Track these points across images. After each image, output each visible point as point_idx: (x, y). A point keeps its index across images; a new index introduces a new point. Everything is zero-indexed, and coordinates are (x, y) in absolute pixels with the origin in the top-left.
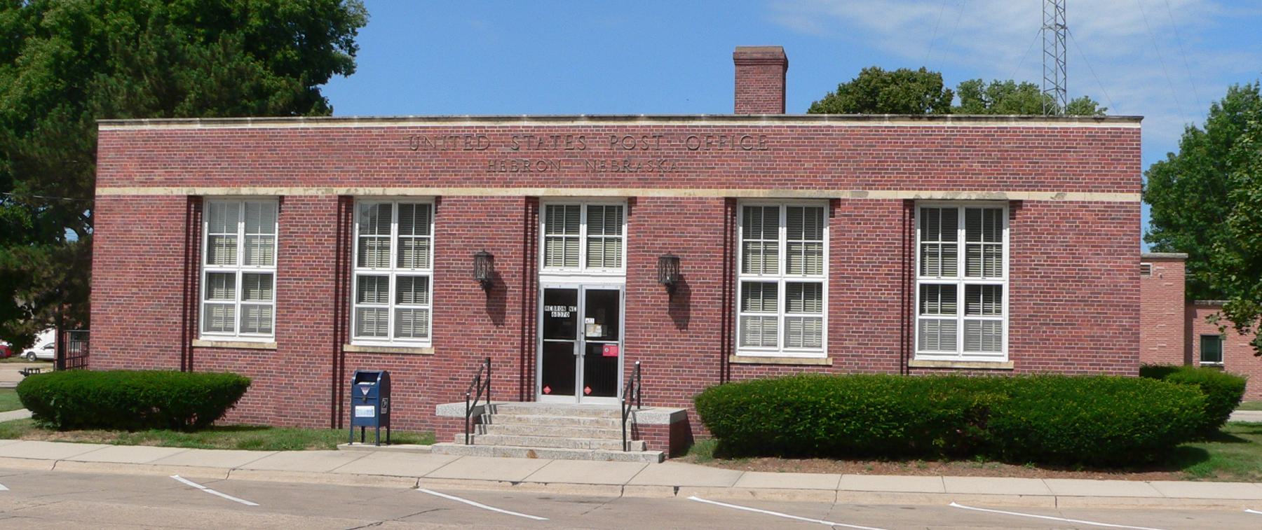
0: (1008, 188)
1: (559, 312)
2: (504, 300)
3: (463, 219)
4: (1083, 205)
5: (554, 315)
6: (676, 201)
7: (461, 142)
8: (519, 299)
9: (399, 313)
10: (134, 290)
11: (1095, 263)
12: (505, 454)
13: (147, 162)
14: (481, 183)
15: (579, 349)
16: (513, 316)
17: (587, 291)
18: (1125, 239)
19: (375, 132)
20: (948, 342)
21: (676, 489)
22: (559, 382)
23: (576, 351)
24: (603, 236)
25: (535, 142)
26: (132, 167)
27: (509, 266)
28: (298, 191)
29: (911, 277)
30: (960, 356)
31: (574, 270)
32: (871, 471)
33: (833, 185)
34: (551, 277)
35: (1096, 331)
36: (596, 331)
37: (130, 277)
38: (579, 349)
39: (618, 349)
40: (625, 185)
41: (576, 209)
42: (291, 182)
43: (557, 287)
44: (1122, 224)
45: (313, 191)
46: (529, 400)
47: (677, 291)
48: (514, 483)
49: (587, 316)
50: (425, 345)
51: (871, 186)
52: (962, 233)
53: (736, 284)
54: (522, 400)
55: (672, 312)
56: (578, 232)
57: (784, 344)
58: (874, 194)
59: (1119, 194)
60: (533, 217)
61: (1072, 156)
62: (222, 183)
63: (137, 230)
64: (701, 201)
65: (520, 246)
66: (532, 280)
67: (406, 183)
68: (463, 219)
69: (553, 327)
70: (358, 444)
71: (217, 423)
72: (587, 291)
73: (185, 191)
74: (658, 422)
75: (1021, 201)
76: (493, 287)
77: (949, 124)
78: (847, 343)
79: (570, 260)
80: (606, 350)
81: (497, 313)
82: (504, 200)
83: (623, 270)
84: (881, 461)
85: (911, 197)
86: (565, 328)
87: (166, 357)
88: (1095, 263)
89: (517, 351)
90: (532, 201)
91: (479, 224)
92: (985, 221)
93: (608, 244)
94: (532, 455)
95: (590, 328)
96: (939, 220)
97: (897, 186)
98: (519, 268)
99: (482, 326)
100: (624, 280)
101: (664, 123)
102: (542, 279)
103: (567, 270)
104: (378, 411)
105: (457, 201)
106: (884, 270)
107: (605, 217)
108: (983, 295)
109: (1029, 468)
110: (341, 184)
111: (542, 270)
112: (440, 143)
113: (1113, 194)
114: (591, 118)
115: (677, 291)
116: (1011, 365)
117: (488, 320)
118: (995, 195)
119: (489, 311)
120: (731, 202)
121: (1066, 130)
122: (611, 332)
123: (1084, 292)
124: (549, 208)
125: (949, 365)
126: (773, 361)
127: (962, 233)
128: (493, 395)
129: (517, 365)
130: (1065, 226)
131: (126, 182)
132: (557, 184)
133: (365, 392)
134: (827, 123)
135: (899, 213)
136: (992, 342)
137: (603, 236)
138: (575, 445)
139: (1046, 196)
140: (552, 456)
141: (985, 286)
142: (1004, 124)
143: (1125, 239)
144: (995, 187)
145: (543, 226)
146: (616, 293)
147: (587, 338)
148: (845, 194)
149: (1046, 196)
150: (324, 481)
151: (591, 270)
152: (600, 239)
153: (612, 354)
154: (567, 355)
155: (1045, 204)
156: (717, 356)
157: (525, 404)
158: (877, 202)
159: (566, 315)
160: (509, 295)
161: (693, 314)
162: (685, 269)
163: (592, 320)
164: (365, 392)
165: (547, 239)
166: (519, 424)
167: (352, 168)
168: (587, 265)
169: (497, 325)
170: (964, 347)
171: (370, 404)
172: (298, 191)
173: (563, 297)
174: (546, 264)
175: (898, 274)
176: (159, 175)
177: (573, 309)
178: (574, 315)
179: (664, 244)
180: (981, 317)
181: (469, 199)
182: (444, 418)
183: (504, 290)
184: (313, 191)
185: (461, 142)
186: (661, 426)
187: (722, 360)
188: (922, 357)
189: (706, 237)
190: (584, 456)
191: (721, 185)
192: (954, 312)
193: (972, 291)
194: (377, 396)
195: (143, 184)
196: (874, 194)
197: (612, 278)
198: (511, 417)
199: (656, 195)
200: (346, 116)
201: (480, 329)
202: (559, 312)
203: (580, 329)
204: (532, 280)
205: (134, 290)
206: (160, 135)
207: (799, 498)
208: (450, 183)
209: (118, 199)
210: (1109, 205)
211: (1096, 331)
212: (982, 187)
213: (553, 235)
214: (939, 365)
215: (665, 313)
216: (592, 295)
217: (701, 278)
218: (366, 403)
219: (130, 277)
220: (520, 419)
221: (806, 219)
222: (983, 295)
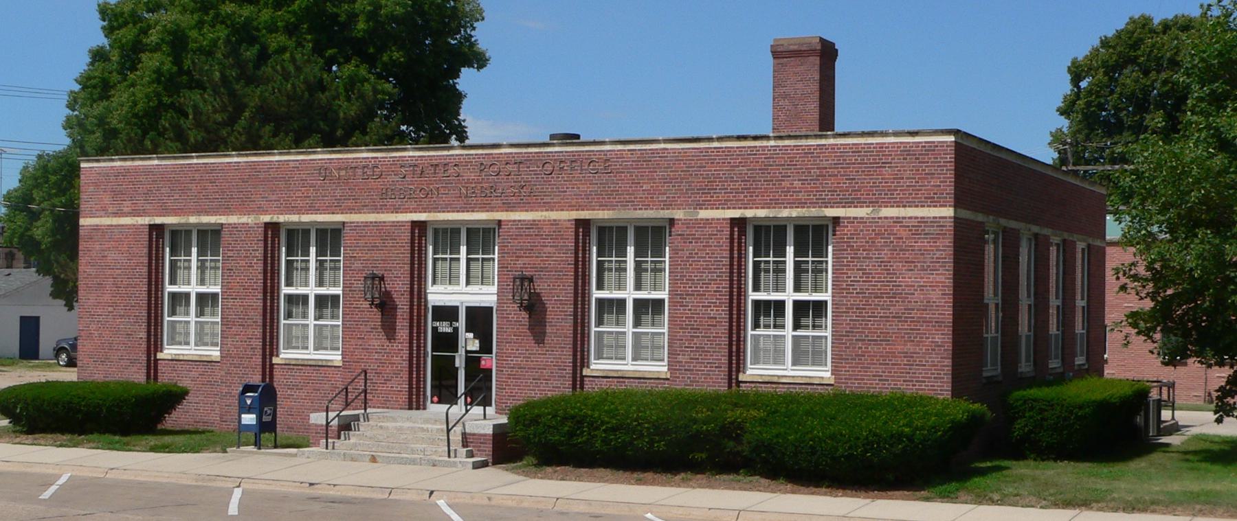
0: (826, 205)
1: (445, 328)
2: (394, 316)
3: (361, 243)
4: (898, 220)
5: (441, 330)
6: (534, 224)
7: (359, 172)
8: (406, 316)
9: (319, 329)
11: (908, 278)
12: (352, 460)
13: (117, 194)
14: (376, 209)
15: (460, 362)
16: (402, 333)
18: (938, 254)
19: (292, 164)
20: (778, 358)
21: (432, 493)
22: (445, 393)
23: (457, 365)
24: (480, 256)
25: (418, 170)
26: (107, 199)
27: (398, 286)
28: (233, 219)
29: (742, 293)
30: (788, 371)
32: (639, 482)
33: (668, 206)
34: (438, 295)
35: (910, 347)
36: (474, 345)
37: (107, 297)
38: (460, 362)
39: (490, 361)
40: (491, 209)
41: (458, 231)
42: (227, 211)
43: (441, 304)
44: (935, 240)
46: (418, 409)
47: (534, 307)
48: (311, 484)
49: (467, 331)
50: (336, 357)
51: (701, 206)
52: (790, 250)
53: (589, 301)
54: (410, 408)
55: (531, 328)
56: (459, 253)
57: (632, 359)
58: (704, 214)
59: (932, 209)
60: (420, 240)
61: (887, 171)
62: (175, 213)
63: (112, 256)
64: (555, 223)
65: (407, 267)
66: (419, 298)
67: (318, 211)
68: (361, 243)
70: (251, 448)
73: (146, 220)
74: (482, 432)
75: (838, 218)
76: (385, 305)
78: (680, 358)
79: (452, 279)
80: (483, 362)
81: (389, 330)
82: (396, 224)
84: (656, 472)
85: (737, 216)
86: (447, 342)
87: (134, 369)
88: (908, 278)
89: (406, 364)
90: (419, 226)
91: (374, 248)
92: (812, 237)
93: (486, 263)
94: (374, 459)
96: (769, 236)
97: (725, 205)
98: (407, 288)
99: (377, 341)
100: (495, 298)
101: (524, 150)
102: (430, 297)
103: (450, 288)
104: (259, 418)
105: (357, 226)
106: (713, 287)
107: (481, 238)
108: (807, 312)
109: (781, 484)
110: (266, 212)
111: (431, 289)
112: (343, 173)
113: (926, 209)
115: (534, 307)
117: (382, 336)
118: (813, 212)
119: (383, 327)
120: (583, 225)
121: (881, 145)
122: (486, 347)
123: (898, 308)
124: (436, 231)
125: (775, 380)
126: (620, 374)
127: (790, 250)
128: (370, 403)
129: (406, 376)
130: (880, 242)
131: (102, 213)
132: (436, 209)
133: (249, 402)
135: (727, 232)
136: (818, 359)
137: (480, 256)
138: (413, 451)
139: (862, 212)
140: (389, 461)
141: (814, 302)
142: (823, 142)
143: (938, 254)
145: (430, 248)
146: (491, 309)
147: (467, 352)
148: (678, 214)
149: (862, 212)
150: (173, 481)
151: (471, 289)
152: (446, 259)
153: (488, 366)
154: (444, 366)
155: (861, 220)
156: (569, 370)
157: (414, 412)
158: (707, 222)
159: (449, 330)
160: (399, 312)
161: (549, 330)
162: (541, 286)
163: (471, 335)
164: (249, 402)
165: (435, 260)
166: (381, 432)
168: (468, 283)
169: (389, 339)
170: (783, 362)
171: (266, 414)
172: (233, 219)
173: (446, 313)
174: (434, 282)
175: (726, 291)
177: (456, 324)
178: (456, 329)
179: (522, 264)
180: (810, 333)
181: (367, 224)
182: (316, 425)
183: (395, 308)
185: (359, 172)
186: (485, 435)
187: (574, 373)
188: (754, 371)
189: (560, 256)
190: (413, 462)
191: (572, 207)
192: (783, 327)
193: (800, 307)
194: (257, 405)
195: (116, 214)
196: (704, 214)
197: (486, 295)
198: (389, 424)
199: (517, 218)
201: (376, 343)
203: (461, 343)
204: (419, 298)
205: (110, 309)
206: (127, 171)
207: (525, 504)
208: (351, 210)
209: (96, 228)
210: (923, 220)
211: (910, 347)
212: (802, 204)
213: (440, 256)
214: (767, 379)
215: (525, 329)
216: (471, 311)
217: (556, 295)
218: (249, 412)
219: (107, 297)
220: (381, 427)
222: (807, 312)
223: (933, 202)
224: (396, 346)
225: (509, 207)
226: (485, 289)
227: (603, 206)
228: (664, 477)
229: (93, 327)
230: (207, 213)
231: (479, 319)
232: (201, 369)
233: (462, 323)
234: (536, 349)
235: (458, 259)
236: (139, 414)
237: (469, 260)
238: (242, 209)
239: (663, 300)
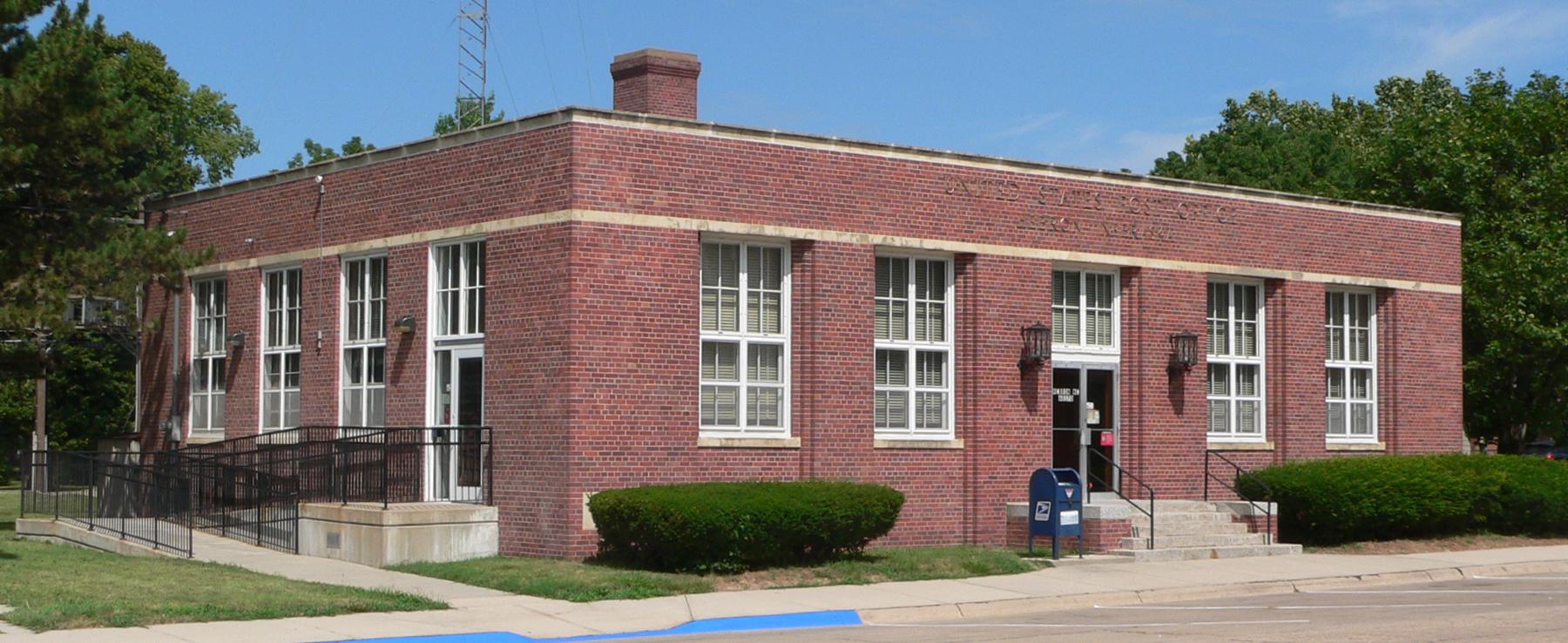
1: (1065, 396)
4: (1431, 294)
5: (1062, 399)
6: (1171, 274)
10: (631, 366)
11: (1438, 350)
12: (1194, 558)
14: (1014, 241)
17: (1089, 372)
19: (910, 167)
26: (623, 182)
28: (830, 236)
31: (1086, 347)
33: (1280, 266)
34: (1063, 354)
36: (1094, 418)
39: (1113, 437)
42: (823, 222)
45: (846, 237)
51: (1304, 268)
62: (742, 217)
63: (633, 277)
64: (1190, 274)
69: (1066, 415)
71: (875, 546)
72: (1089, 372)
73: (693, 224)
77: (1352, 210)
82: (1035, 262)
83: (1116, 348)
86: (1066, 415)
87: (676, 464)
94: (1214, 555)
95: (1090, 415)
99: (1017, 413)
100: (1117, 360)
102: (1054, 357)
103: (1073, 347)
110: (876, 230)
111: (1055, 346)
116: (1382, 446)
119: (1023, 395)
122: (1106, 421)
131: (616, 205)
134: (1275, 201)
140: (1229, 554)
144: (1380, 275)
146: (1110, 373)
148: (1288, 275)
159: (1070, 399)
163: (1091, 405)
167: (888, 210)
172: (830, 236)
173: (1066, 377)
176: (660, 197)
177: (1077, 392)
178: (1077, 398)
181: (1003, 260)
182: (1109, 521)
184: (846, 237)
195: (643, 208)
197: (1108, 355)
200: (1087, 168)
201: (1015, 416)
202: (1065, 396)
205: (631, 366)
206: (659, 140)
208: (985, 239)
209: (604, 229)
211: (1438, 414)
216: (1092, 373)
219: (624, 347)
221: (1248, 296)
223: (1451, 282)
224: (1038, 420)
225: (1149, 253)
226: (1106, 349)
227: (1231, 261)
228: (1421, 544)
229: (600, 395)
230: (792, 222)
231: (1100, 382)
232: (765, 460)
233: (1083, 391)
234: (1176, 421)
235: (1078, 312)
236: (818, 530)
237: (1089, 312)
238: (845, 224)
239: (1370, 370)
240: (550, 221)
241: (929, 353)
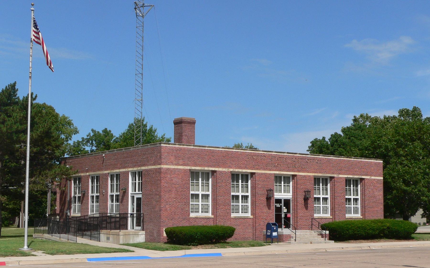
1: (278, 205)
4: (374, 179)
5: (277, 206)
6: (305, 176)
10: (174, 200)
11: (376, 193)
12: (306, 243)
13: (177, 158)
17: (284, 200)
19: (239, 153)
26: (172, 159)
28: (220, 169)
31: (283, 193)
33: (333, 173)
34: (277, 195)
37: (173, 195)
39: (290, 215)
42: (219, 166)
45: (224, 170)
51: (340, 174)
58: (341, 176)
61: (372, 168)
62: (200, 166)
63: (175, 180)
64: (309, 176)
69: (278, 210)
71: (228, 240)
72: (284, 200)
73: (188, 168)
77: (353, 159)
79: (280, 191)
82: (270, 174)
83: (291, 194)
86: (278, 210)
94: (311, 243)
95: (285, 210)
99: (266, 210)
100: (291, 197)
102: (275, 196)
110: (231, 168)
111: (275, 194)
114: (288, 153)
116: (362, 217)
122: (289, 211)
131: (171, 164)
134: (332, 158)
140: (315, 243)
144: (360, 175)
146: (290, 200)
148: (335, 176)
159: (279, 206)
163: (285, 208)
167: (234, 163)
172: (220, 169)
173: (278, 201)
176: (181, 162)
177: (281, 204)
178: (281, 206)
181: (262, 174)
184: (224, 170)
195: (176, 165)
197: (289, 196)
202: (278, 205)
205: (174, 200)
206: (181, 149)
208: (257, 169)
209: (168, 169)
211: (377, 209)
212: (358, 175)
216: (285, 200)
219: (173, 195)
221: (325, 181)
223: (380, 176)
224: (271, 211)
225: (299, 171)
226: (288, 194)
227: (320, 173)
228: (366, 241)
229: (167, 206)
230: (211, 167)
231: (287, 203)
232: (205, 221)
233: (283, 204)
234: (306, 211)
235: (281, 185)
236: (217, 236)
237: (284, 186)
238: (224, 166)
240: (156, 167)
241: (245, 196)
